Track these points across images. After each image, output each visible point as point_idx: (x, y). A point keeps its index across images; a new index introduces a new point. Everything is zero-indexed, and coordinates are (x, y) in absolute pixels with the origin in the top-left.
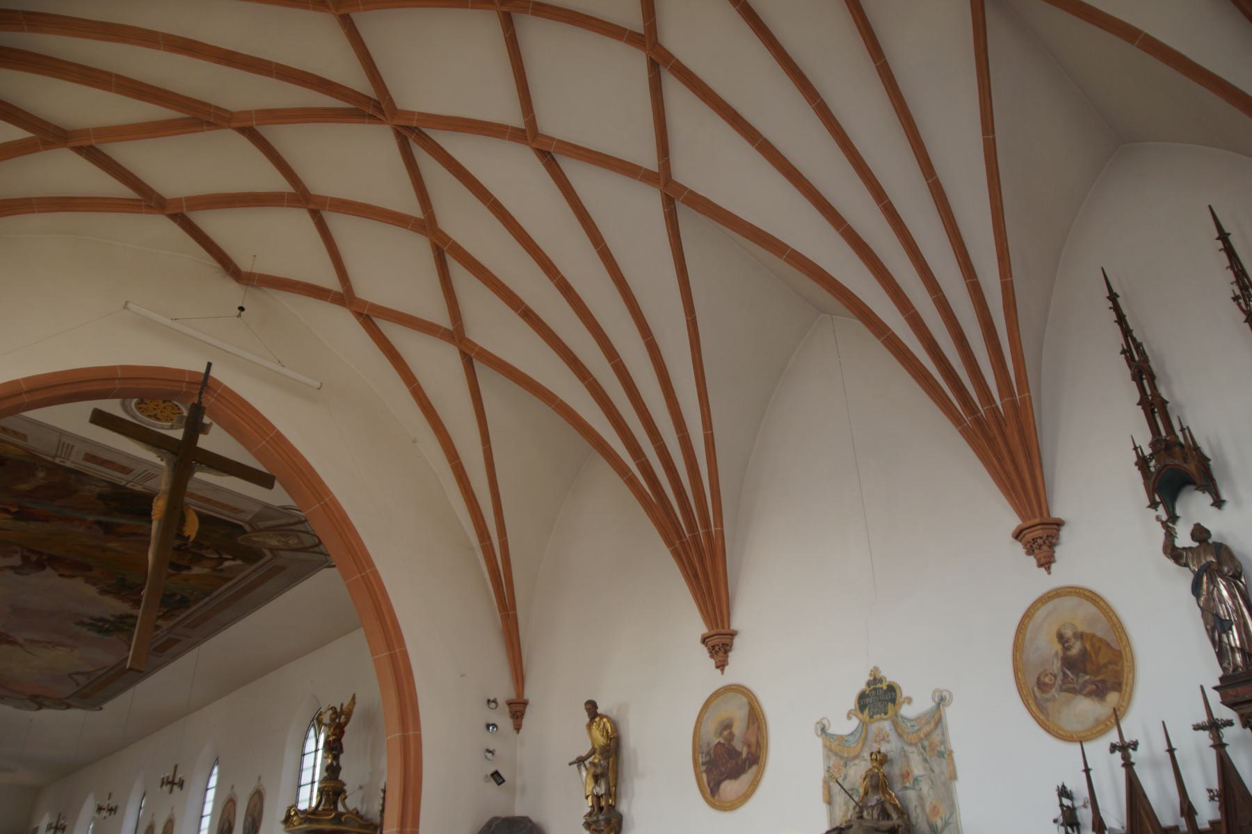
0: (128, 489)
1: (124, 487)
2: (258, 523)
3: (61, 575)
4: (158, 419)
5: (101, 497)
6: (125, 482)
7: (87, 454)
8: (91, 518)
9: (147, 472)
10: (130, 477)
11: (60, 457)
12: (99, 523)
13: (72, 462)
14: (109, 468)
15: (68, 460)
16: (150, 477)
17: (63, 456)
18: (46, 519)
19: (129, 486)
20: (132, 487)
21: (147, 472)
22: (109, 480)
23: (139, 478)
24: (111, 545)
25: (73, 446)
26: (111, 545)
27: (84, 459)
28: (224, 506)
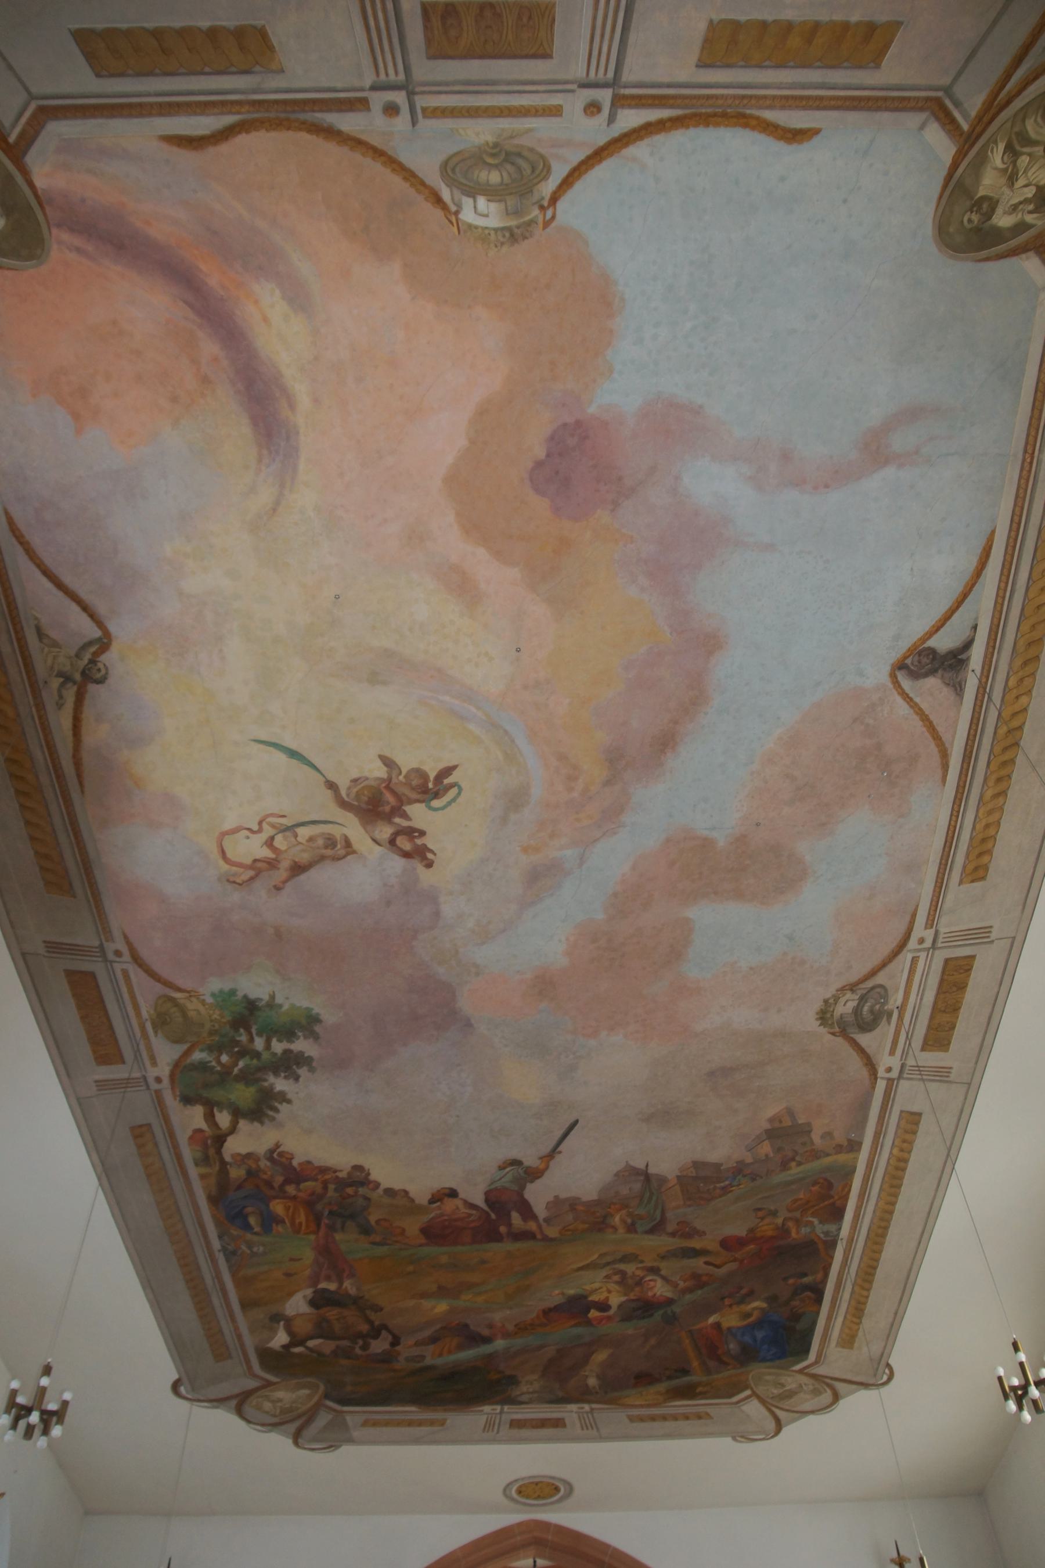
0: (497, 1403)
2: (330, 1417)
3: (453, 1193)
4: (532, 1483)
8: (500, 1344)
9: (495, 1430)
11: (587, 1413)
12: (487, 1340)
14: (533, 1420)
15: (576, 1412)
16: (488, 1426)
17: (585, 1416)
18: (546, 1312)
19: (498, 1408)
21: (495, 1430)
22: (523, 1406)
23: (497, 1421)
24: (442, 1307)
25: (583, 1429)
26: (442, 1307)
28: (387, 1424)
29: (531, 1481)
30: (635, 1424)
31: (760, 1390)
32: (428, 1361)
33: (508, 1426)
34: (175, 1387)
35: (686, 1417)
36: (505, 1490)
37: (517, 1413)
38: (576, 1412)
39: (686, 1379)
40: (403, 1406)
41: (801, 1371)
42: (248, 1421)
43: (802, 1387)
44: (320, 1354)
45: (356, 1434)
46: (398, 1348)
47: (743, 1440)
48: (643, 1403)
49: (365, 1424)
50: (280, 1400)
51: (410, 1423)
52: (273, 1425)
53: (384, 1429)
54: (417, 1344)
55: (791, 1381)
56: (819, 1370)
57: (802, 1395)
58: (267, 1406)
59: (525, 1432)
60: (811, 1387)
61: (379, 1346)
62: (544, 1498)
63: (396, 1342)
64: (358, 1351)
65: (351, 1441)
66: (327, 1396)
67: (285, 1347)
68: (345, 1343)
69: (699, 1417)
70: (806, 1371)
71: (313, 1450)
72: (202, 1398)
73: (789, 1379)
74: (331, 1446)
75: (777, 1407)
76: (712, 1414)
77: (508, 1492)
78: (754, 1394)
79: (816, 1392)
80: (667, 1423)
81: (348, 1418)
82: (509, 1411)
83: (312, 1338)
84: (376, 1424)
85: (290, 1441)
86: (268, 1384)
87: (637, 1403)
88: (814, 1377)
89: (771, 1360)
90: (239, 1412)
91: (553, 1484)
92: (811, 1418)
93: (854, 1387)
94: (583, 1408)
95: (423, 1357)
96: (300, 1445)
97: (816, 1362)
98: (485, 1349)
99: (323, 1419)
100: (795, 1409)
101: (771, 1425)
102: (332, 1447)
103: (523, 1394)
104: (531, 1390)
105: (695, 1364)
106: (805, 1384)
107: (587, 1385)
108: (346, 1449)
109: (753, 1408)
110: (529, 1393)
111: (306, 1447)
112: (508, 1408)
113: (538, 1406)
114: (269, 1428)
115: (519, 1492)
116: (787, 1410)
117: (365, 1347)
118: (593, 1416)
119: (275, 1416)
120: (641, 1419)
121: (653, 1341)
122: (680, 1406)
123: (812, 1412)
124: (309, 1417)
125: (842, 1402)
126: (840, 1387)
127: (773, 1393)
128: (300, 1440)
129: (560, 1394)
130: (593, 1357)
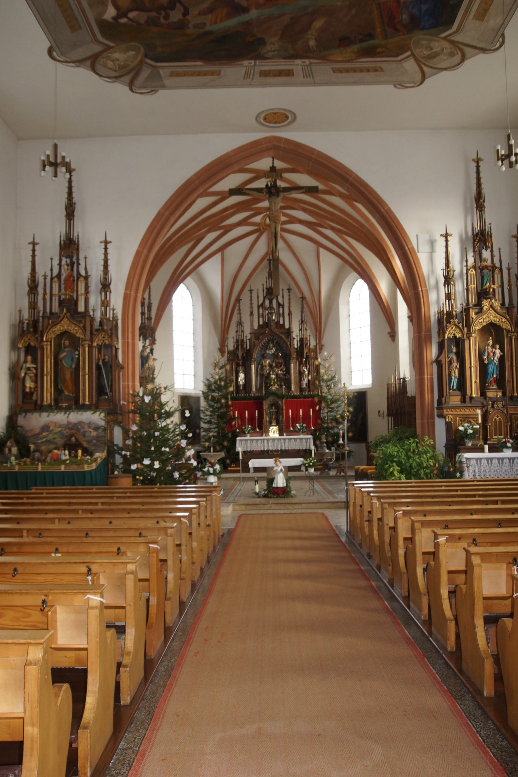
0: (251, 59)
1: (255, 58)
2: (149, 71)
4: (273, 113)
5: (262, 42)
6: (257, 63)
7: (293, 75)
8: (254, 13)
10: (258, 69)
11: (307, 66)
12: (245, 10)
13: (298, 65)
14: (274, 70)
15: (301, 65)
16: (247, 75)
19: (253, 62)
20: (251, 61)
25: (304, 77)
27: (293, 70)
28: (185, 74)
29: (271, 112)
30: (335, 74)
31: (417, 52)
32: (208, 28)
33: (259, 75)
34: (50, 52)
35: (368, 70)
36: (256, 118)
37: (264, 65)
38: (301, 65)
39: (371, 42)
40: (194, 61)
41: (445, 38)
42: (100, 76)
43: (443, 50)
44: (138, 23)
45: (167, 82)
46: (188, 17)
47: (400, 87)
48: (342, 59)
49: (172, 75)
50: (117, 60)
51: (199, 74)
52: (116, 78)
53: (184, 78)
54: (200, 14)
55: (438, 45)
56: (458, 38)
57: (442, 56)
58: (110, 64)
59: (269, 80)
60: (449, 50)
61: (176, 16)
62: (279, 123)
63: (186, 13)
64: (163, 21)
65: (164, 87)
66: (146, 56)
67: (115, 18)
68: (154, 14)
69: (376, 70)
70: (448, 38)
71: (141, 93)
72: (68, 60)
73: (437, 44)
74: (152, 91)
75: (425, 65)
76: (384, 68)
77: (258, 119)
78: (413, 55)
79: (452, 54)
80: (356, 74)
81: (161, 71)
82: (260, 64)
83: (131, 10)
84: (178, 75)
85: (127, 88)
86: (108, 48)
87: (339, 59)
88: (453, 43)
89: (428, 29)
90: (94, 69)
91: (285, 114)
92: (444, 73)
93: (477, 51)
94: (305, 62)
95: (204, 24)
96: (134, 90)
97: (457, 32)
98: (245, 18)
99: (145, 73)
100: (436, 66)
101: (419, 77)
102: (153, 91)
103: (269, 51)
104: (273, 49)
105: (379, 30)
106: (446, 48)
107: (308, 46)
108: (161, 93)
109: (410, 65)
110: (272, 51)
111: (137, 91)
112: (259, 62)
113: (277, 61)
114: (114, 80)
115: (265, 119)
116: (431, 67)
117: (167, 17)
118: (311, 68)
119: (115, 71)
120: (340, 71)
121: (353, 12)
122: (366, 62)
123: (446, 69)
124: (136, 71)
125: (466, 62)
126: (467, 50)
127: (424, 54)
128: (133, 87)
129: (291, 52)
130: (314, 24)
